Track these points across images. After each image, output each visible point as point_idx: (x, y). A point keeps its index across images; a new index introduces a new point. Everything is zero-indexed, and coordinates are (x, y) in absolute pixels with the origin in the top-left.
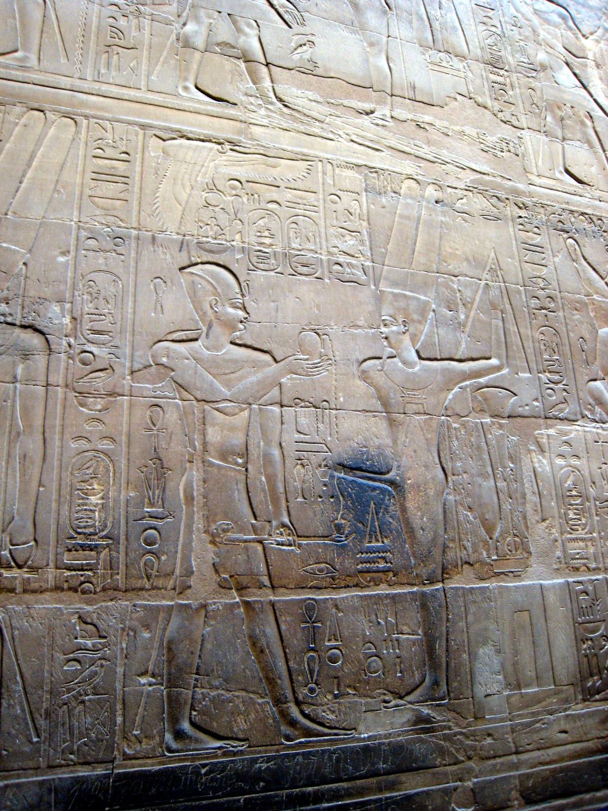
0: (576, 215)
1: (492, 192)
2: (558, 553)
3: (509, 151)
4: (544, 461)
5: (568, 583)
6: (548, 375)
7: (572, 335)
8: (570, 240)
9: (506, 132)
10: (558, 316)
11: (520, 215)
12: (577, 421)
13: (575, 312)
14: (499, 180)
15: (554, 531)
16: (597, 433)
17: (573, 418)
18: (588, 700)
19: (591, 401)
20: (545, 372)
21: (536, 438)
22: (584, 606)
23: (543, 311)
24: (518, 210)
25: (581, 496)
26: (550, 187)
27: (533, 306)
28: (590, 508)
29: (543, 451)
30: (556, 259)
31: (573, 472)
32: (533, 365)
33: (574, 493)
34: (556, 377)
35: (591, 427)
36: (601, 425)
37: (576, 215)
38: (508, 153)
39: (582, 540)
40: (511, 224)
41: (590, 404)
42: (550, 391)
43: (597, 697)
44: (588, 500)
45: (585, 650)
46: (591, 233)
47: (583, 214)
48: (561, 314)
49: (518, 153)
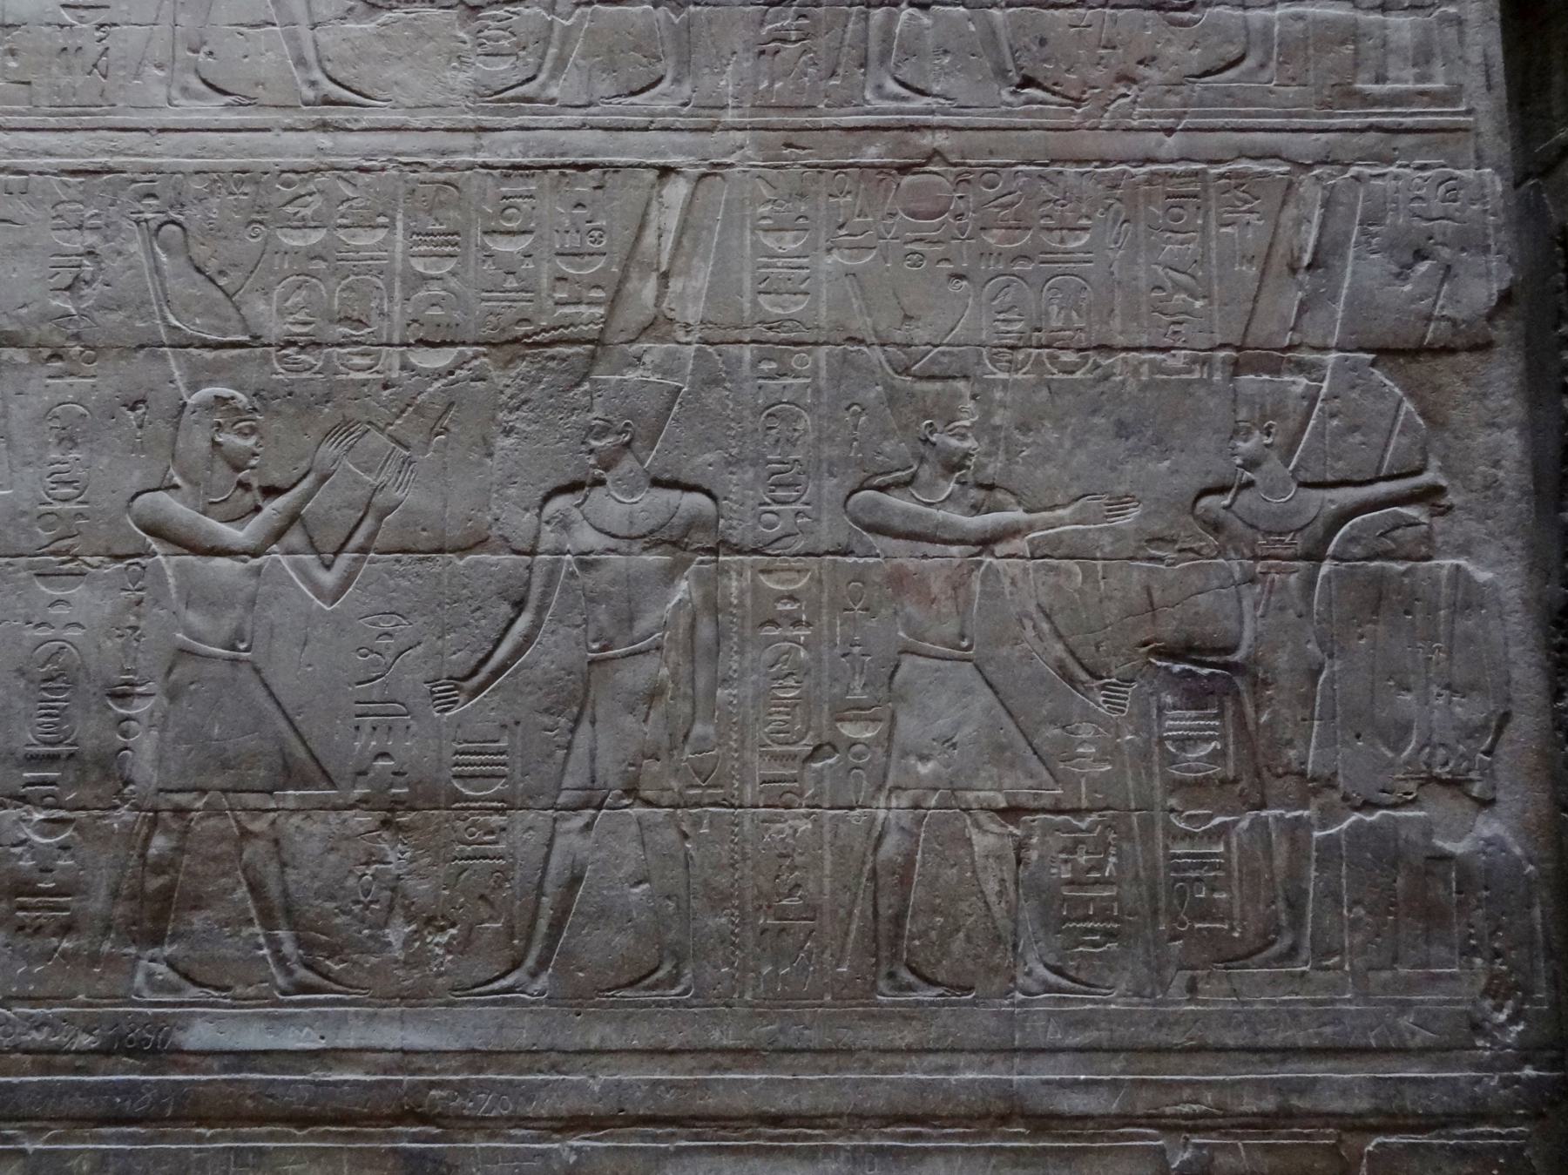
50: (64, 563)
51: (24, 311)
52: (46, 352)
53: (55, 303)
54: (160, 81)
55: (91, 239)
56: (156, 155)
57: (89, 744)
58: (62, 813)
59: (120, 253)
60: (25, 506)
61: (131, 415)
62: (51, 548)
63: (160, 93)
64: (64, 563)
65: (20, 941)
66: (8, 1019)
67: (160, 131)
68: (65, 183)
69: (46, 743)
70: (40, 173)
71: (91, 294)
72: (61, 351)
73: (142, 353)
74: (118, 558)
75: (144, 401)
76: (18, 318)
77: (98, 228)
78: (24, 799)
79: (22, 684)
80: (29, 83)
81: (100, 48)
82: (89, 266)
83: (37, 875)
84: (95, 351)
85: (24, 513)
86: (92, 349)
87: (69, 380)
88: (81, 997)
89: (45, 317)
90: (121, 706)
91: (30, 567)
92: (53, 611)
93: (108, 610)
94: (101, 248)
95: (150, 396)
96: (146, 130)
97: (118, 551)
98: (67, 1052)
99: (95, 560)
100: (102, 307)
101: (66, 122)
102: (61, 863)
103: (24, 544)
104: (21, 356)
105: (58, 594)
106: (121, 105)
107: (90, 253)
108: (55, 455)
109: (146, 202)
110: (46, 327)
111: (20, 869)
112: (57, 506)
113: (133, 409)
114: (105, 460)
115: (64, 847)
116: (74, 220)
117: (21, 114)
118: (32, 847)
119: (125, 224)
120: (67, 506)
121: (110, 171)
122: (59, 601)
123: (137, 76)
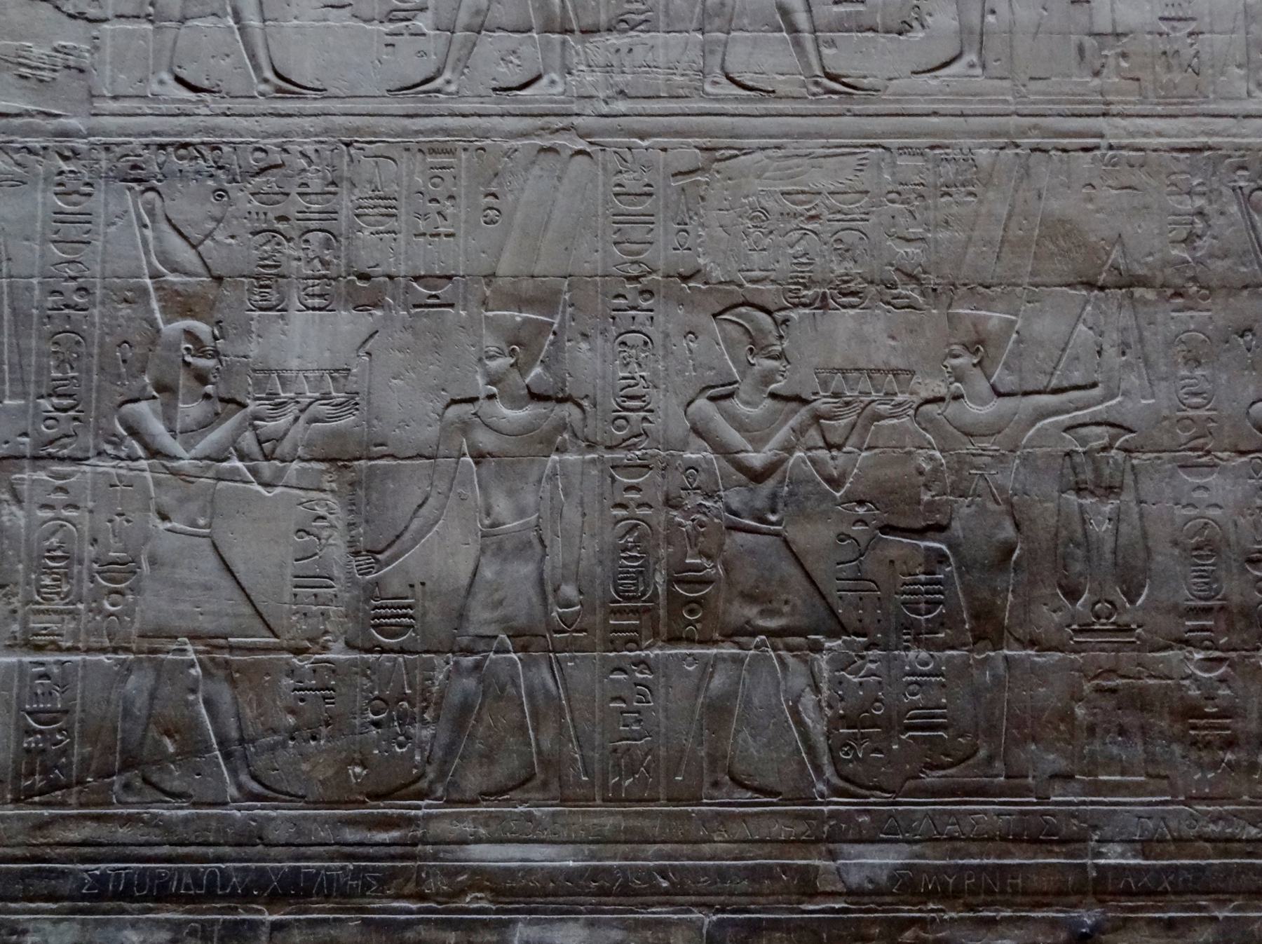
0: (170, 149)
1: (19, 141)
2: (16, 627)
3: (68, 67)
4: (20, 513)
5: (21, 663)
6: (55, 400)
7: (108, 339)
8: (151, 195)
9: (72, 36)
10: (92, 315)
11: (65, 168)
12: (88, 459)
13: (124, 305)
14: (38, 120)
15: (13, 600)
16: (118, 475)
17: (80, 455)
18: (22, 801)
19: (121, 430)
20: (50, 395)
21: (12, 484)
22: (39, 692)
23: (67, 311)
24: (61, 163)
25: (67, 558)
26: (131, 112)
27: (50, 306)
28: (80, 572)
29: (18, 501)
30: (113, 228)
31: (62, 526)
32: (32, 389)
33: (59, 553)
34: (66, 402)
35: (106, 466)
36: (129, 463)
37: (170, 149)
38: (67, 71)
39: (55, 612)
40: (41, 185)
41: (115, 435)
42: (50, 422)
43: (37, 799)
44: (80, 562)
45: (29, 743)
46: (191, 175)
47: (185, 146)
48: (96, 312)
49: (83, 66)
50: (1199, 457)
51: (1150, 259)
52: (1170, 292)
53: (1175, 252)
54: (1241, 78)
55: (1200, 202)
56: (1244, 136)
57: (1236, 599)
58: (1217, 654)
59: (1222, 213)
60: (1165, 412)
61: (1241, 341)
62: (1191, 444)
63: (1241, 87)
64: (1199, 457)
65: (1194, 755)
66: (1191, 815)
67: (1246, 117)
68: (1177, 159)
69: (1200, 598)
70: (1155, 150)
71: (1204, 244)
72: (1182, 291)
73: (1245, 293)
74: (1243, 453)
75: (1250, 330)
76: (1146, 264)
77: (1204, 194)
78: (1187, 642)
79: (1176, 552)
80: (1138, 80)
81: (1193, 52)
82: (1199, 225)
83: (1203, 702)
84: (1209, 290)
85: (1165, 418)
86: (1208, 288)
87: (1189, 313)
88: (1246, 798)
89: (1166, 263)
90: (1255, 569)
91: (1174, 460)
92: (1196, 495)
93: (1239, 495)
94: (1208, 209)
95: (1256, 326)
96: (1234, 116)
97: (1242, 448)
98: (1240, 841)
99: (1225, 455)
100: (1211, 256)
101: (1172, 109)
102: (1220, 692)
103: (1166, 440)
104: (1150, 295)
105: (1198, 481)
106: (1211, 96)
107: (1200, 213)
108: (1184, 372)
109: (1240, 173)
110: (1169, 271)
111: (1191, 697)
112: (1191, 413)
113: (1242, 336)
114: (1224, 377)
115: (1222, 680)
116: (1185, 189)
117: (1135, 104)
118: (1196, 680)
119: (1224, 189)
120: (1198, 412)
121: (1210, 148)
122: (1199, 487)
123: (1222, 74)
